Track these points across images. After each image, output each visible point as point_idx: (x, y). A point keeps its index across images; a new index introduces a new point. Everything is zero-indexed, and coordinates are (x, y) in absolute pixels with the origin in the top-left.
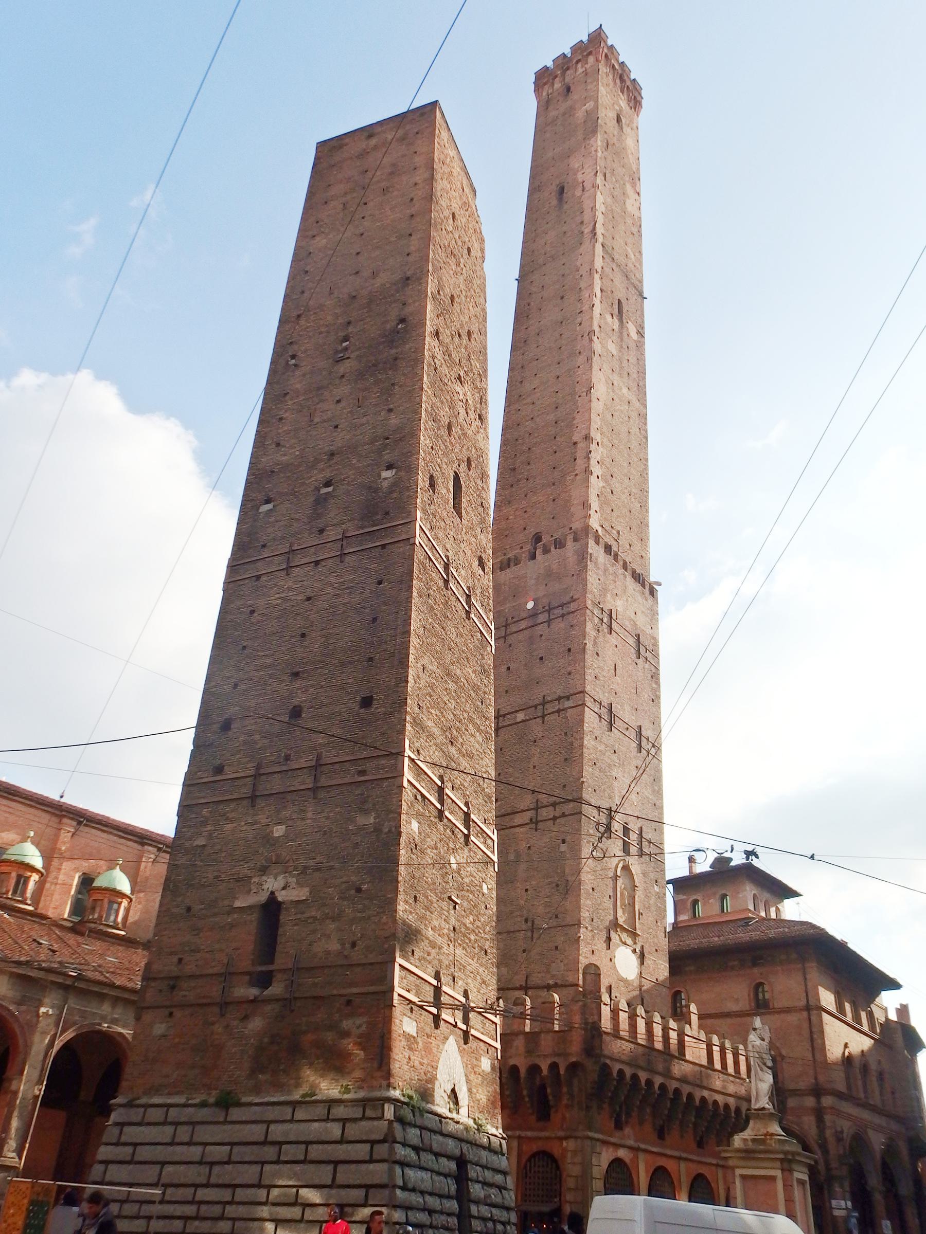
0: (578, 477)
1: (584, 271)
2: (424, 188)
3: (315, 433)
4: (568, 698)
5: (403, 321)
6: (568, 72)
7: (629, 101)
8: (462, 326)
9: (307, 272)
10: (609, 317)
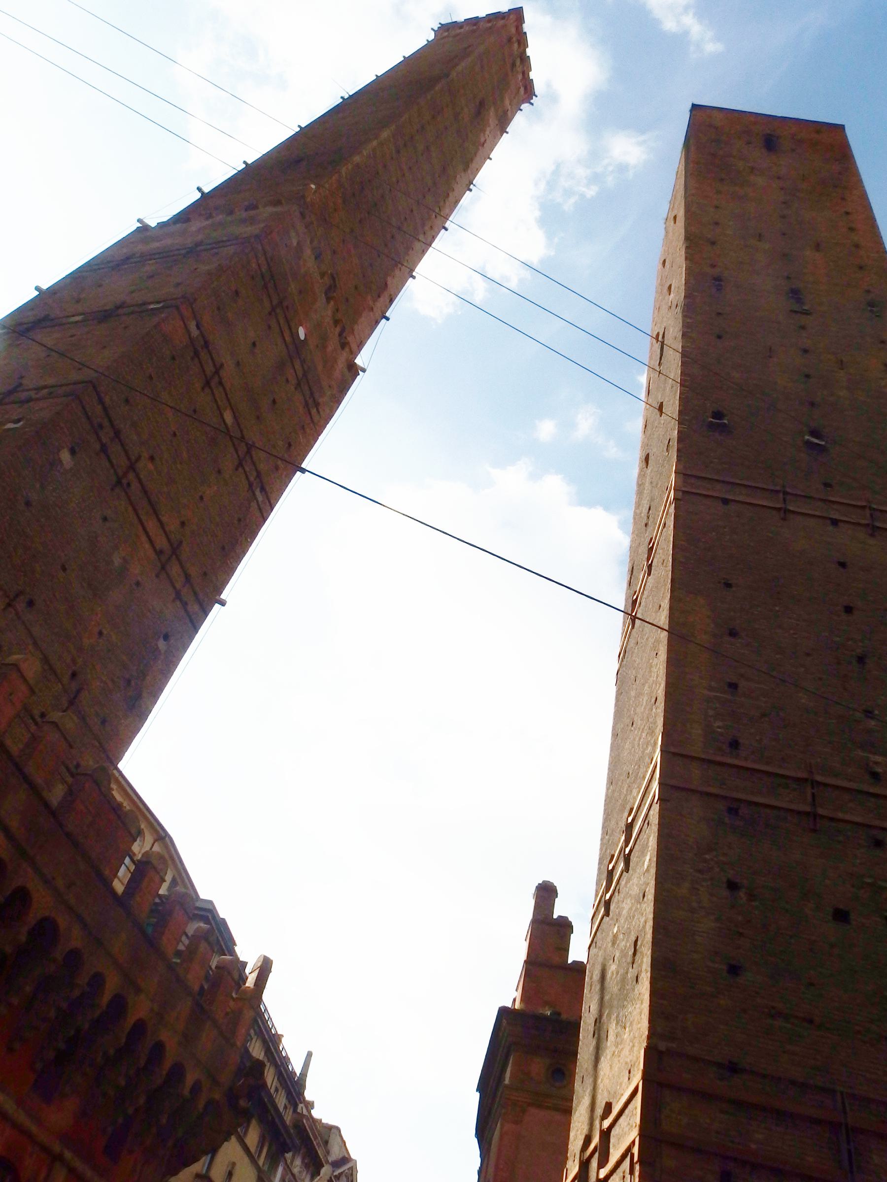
4: (263, 489)
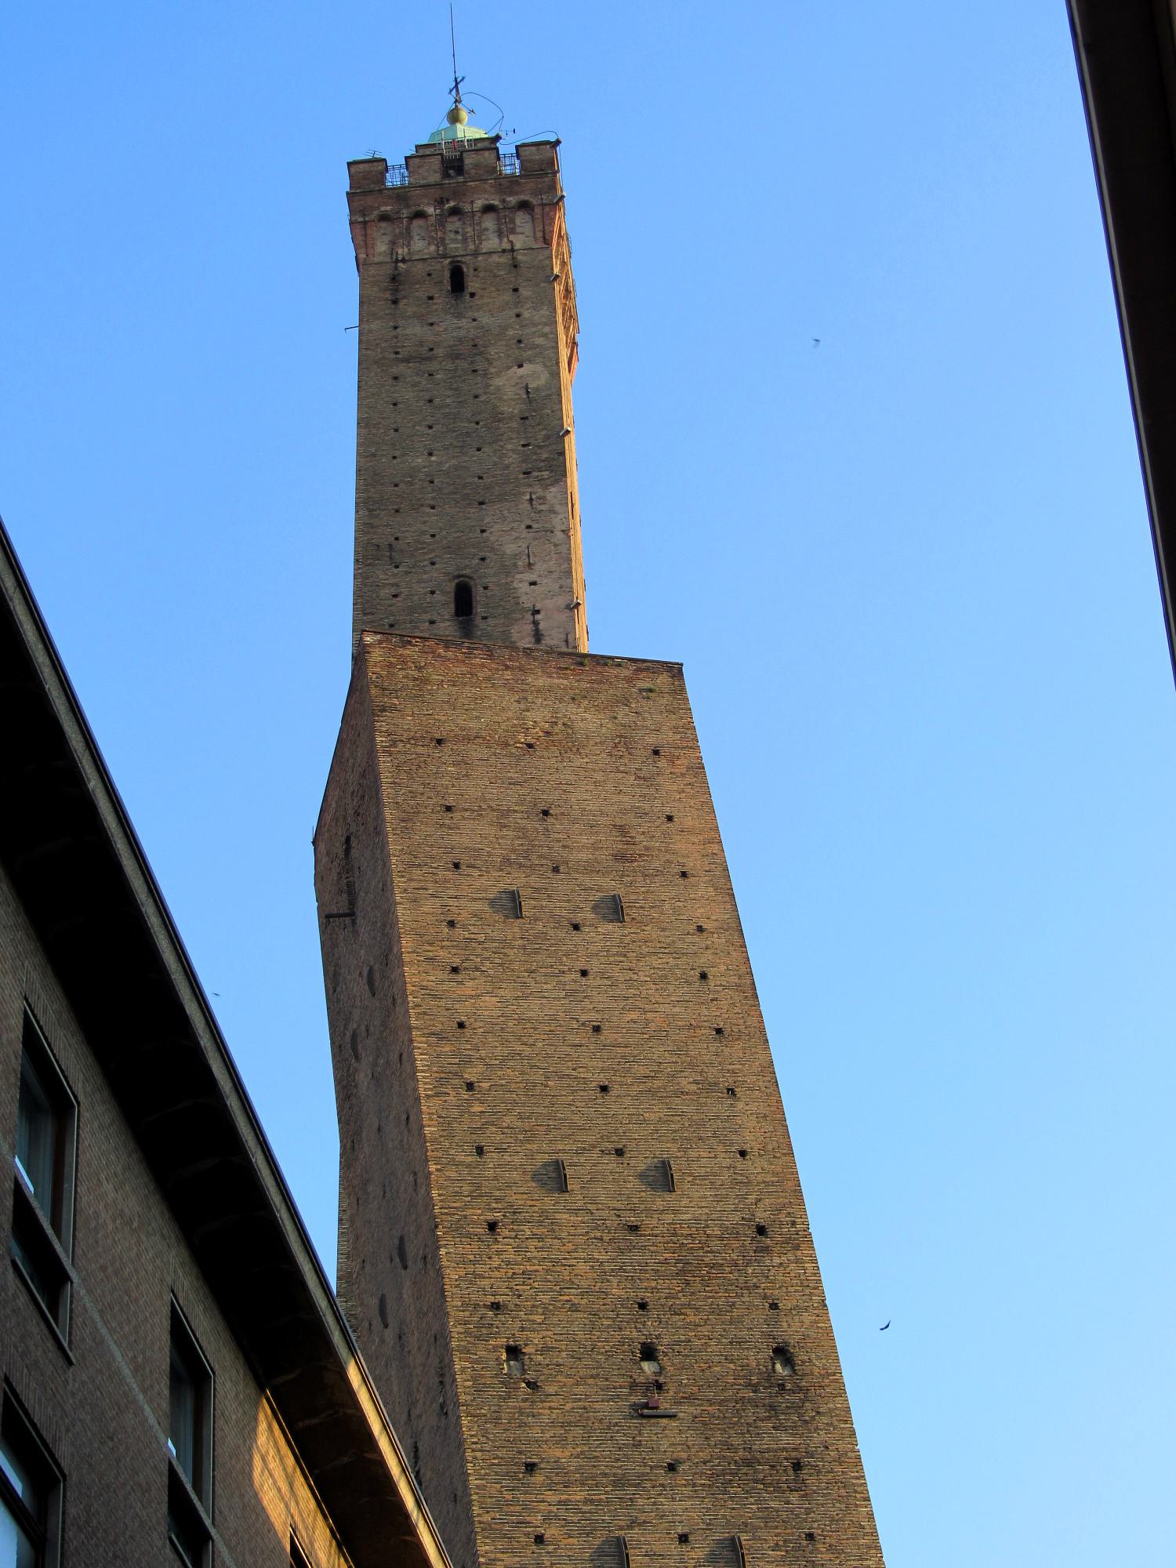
5: (782, 1353)
6: (454, 223)
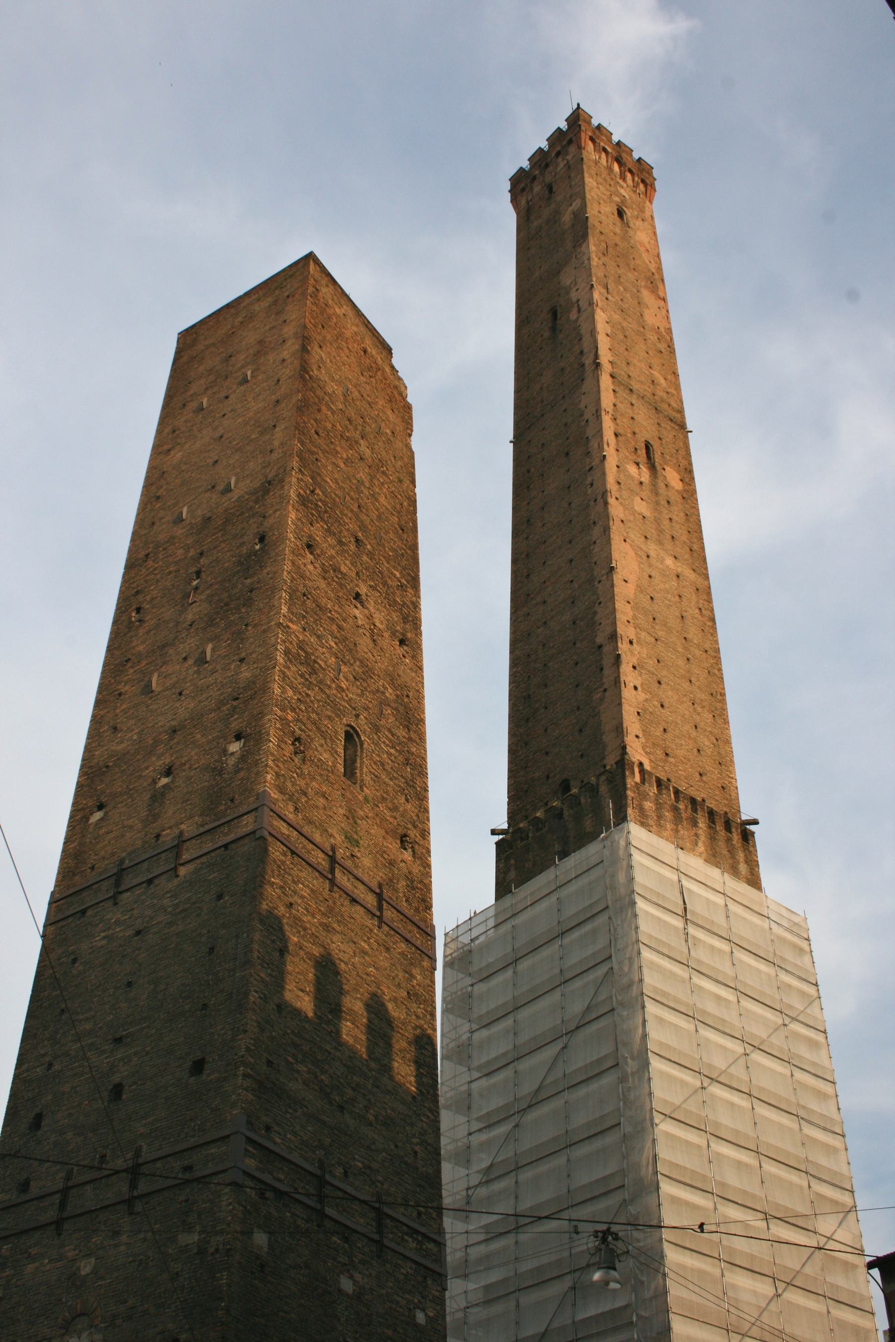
0: (607, 694)
1: (588, 415)
2: (292, 363)
3: (155, 707)
6: (551, 169)
7: (636, 186)
8: (363, 527)
9: (158, 498)
10: (632, 469)
